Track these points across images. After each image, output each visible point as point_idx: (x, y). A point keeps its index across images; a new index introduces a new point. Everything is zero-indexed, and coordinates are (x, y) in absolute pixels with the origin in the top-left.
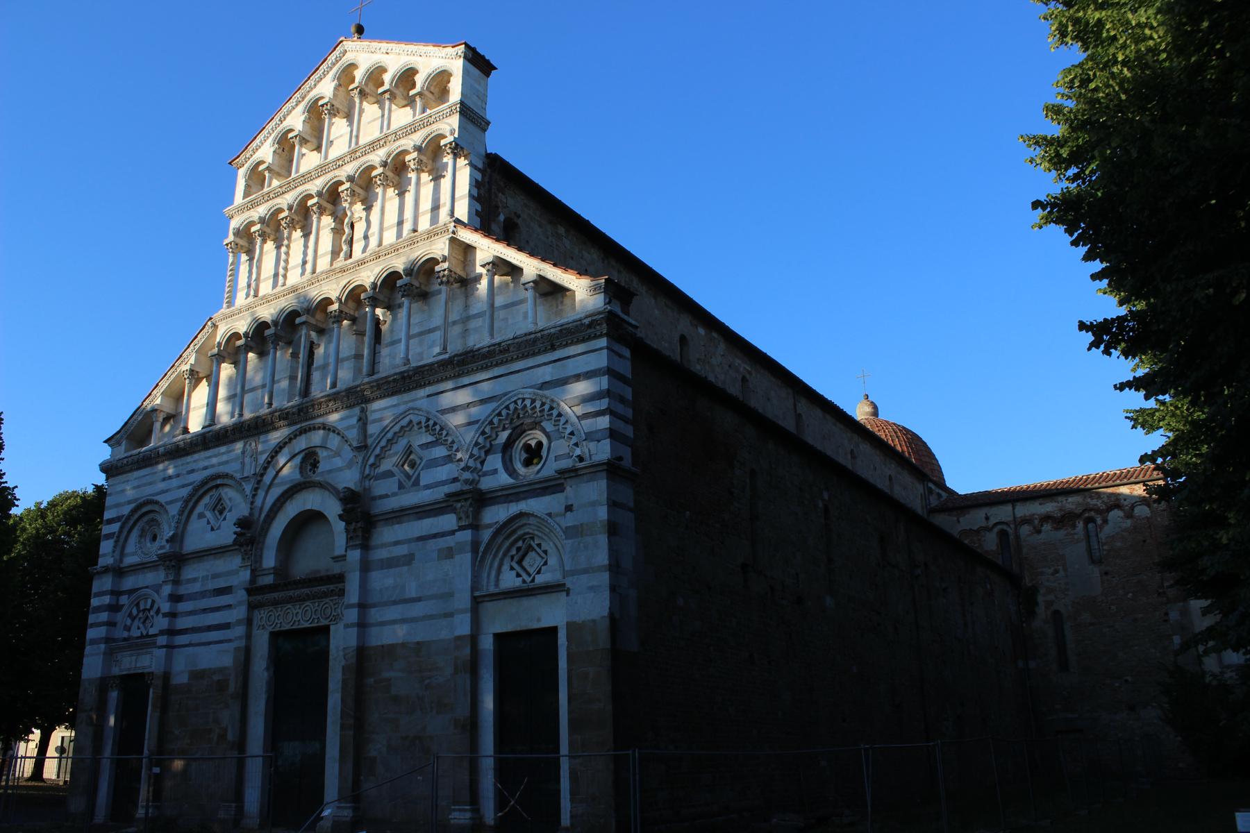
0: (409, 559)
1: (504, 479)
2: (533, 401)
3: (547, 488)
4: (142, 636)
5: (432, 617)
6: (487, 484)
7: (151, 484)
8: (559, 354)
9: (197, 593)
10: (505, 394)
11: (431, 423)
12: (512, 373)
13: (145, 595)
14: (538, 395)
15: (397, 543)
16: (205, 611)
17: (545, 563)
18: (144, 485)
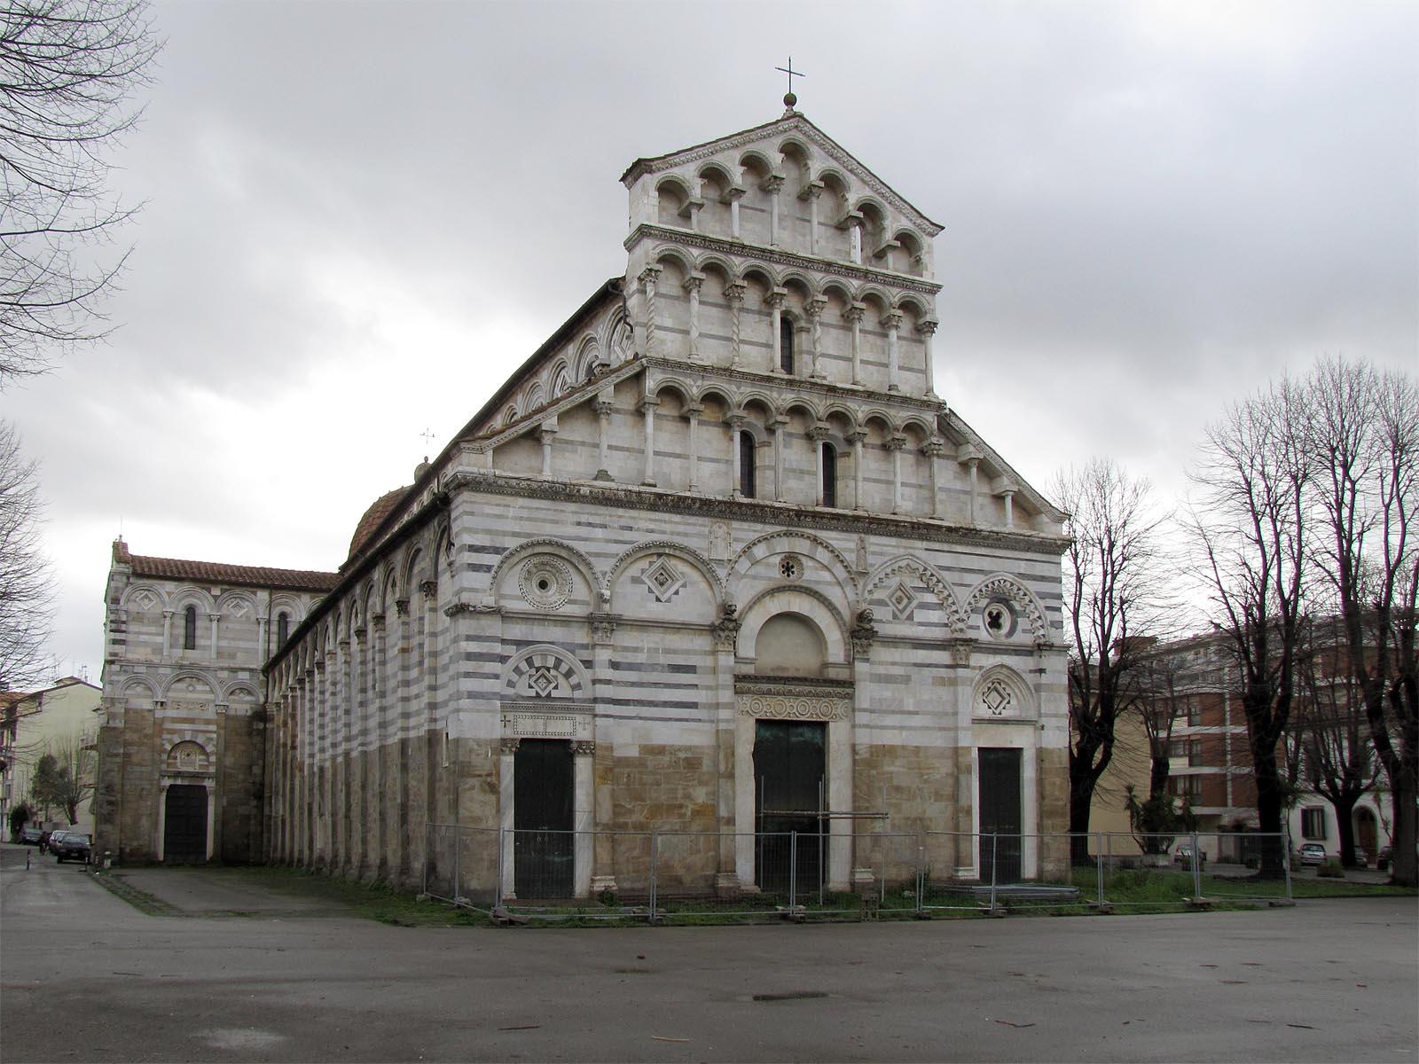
0: (906, 679)
1: (983, 635)
2: (1012, 584)
3: (1015, 650)
4: (538, 696)
5: (927, 728)
6: (971, 634)
7: (556, 522)
8: (1029, 555)
9: (642, 664)
10: (991, 572)
11: (929, 573)
12: (994, 556)
13: (548, 650)
14: (1016, 581)
15: (893, 664)
16: (656, 685)
17: (1009, 703)
18: (544, 521)
